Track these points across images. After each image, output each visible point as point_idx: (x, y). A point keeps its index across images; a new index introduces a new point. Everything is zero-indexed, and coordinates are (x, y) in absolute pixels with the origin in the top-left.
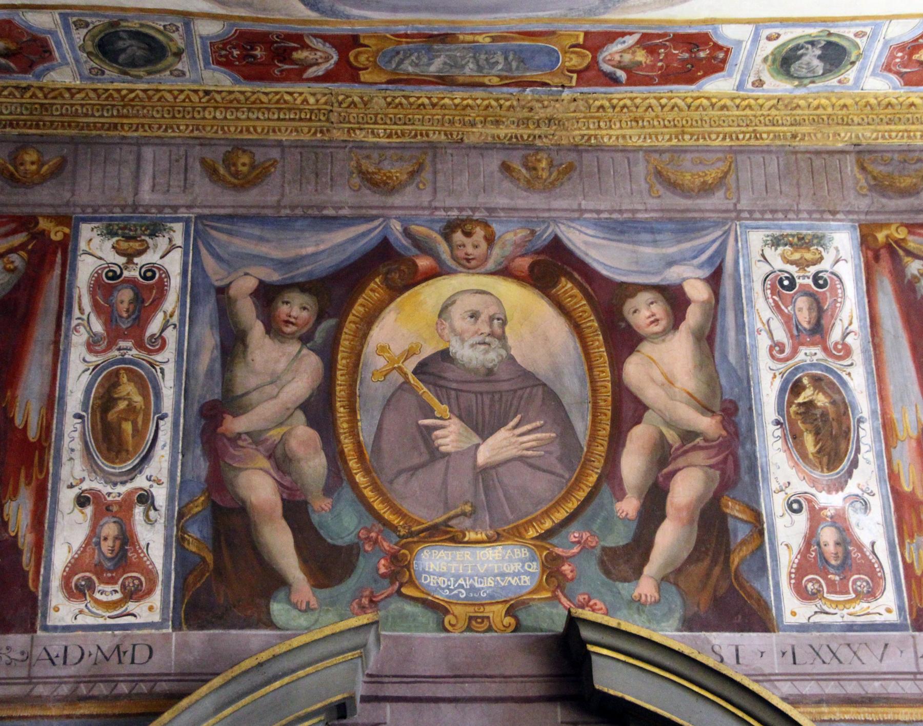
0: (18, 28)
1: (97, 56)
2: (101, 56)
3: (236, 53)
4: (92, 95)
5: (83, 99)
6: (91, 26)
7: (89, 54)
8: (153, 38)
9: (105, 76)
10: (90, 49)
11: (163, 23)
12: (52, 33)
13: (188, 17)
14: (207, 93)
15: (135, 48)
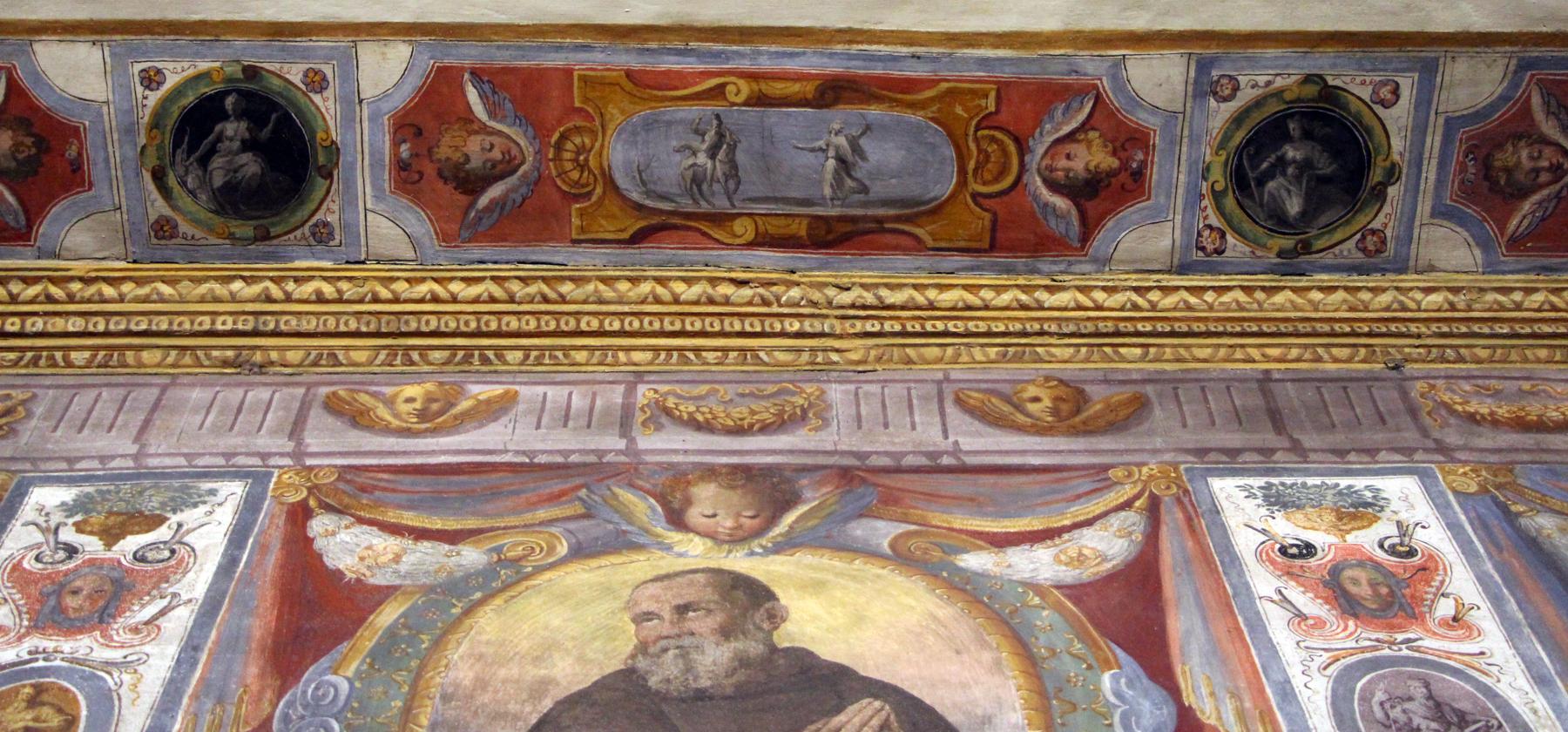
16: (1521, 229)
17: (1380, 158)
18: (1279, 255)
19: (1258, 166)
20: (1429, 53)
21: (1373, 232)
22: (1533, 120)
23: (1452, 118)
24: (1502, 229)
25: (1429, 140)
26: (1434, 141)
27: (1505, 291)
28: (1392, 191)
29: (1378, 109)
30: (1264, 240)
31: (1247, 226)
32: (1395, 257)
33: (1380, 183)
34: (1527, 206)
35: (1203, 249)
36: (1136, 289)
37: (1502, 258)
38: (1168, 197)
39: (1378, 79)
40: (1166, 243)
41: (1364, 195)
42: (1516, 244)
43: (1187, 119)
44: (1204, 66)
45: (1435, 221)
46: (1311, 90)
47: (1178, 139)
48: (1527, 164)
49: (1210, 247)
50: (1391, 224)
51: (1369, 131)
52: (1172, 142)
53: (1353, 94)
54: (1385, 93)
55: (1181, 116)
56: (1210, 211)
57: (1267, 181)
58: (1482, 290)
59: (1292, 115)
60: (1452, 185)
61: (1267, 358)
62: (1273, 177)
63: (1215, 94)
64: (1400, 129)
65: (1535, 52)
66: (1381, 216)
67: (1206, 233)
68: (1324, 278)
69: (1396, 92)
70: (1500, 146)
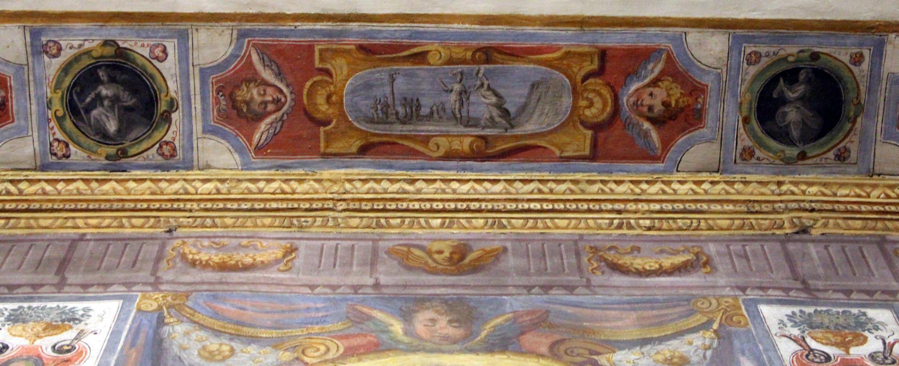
16: (262, 141)
17: (163, 95)
18: (107, 158)
19: (83, 101)
20: (182, 26)
21: (167, 143)
22: (255, 70)
23: (204, 69)
24: (250, 140)
25: (192, 82)
26: (195, 83)
27: (255, 181)
28: (175, 116)
29: (155, 62)
30: (95, 149)
31: (82, 139)
32: (184, 159)
33: (165, 111)
34: (263, 126)
35: (55, 154)
36: (11, 181)
37: (253, 160)
38: (26, 119)
39: (152, 43)
40: (29, 151)
41: (156, 116)
42: (260, 150)
43: (31, 69)
44: (35, 34)
45: (206, 136)
46: (109, 51)
47: (27, 83)
48: (258, 99)
49: (60, 154)
50: (177, 138)
51: (152, 76)
52: (23, 85)
53: (138, 53)
54: (158, 52)
55: (26, 68)
56: (56, 130)
57: (91, 110)
58: (239, 181)
59: (100, 67)
60: (213, 114)
61: (88, 226)
62: (95, 107)
63: (47, 53)
64: (172, 76)
65: (248, 26)
66: (170, 132)
67: (56, 144)
68: (138, 173)
69: (165, 51)
70: (238, 87)
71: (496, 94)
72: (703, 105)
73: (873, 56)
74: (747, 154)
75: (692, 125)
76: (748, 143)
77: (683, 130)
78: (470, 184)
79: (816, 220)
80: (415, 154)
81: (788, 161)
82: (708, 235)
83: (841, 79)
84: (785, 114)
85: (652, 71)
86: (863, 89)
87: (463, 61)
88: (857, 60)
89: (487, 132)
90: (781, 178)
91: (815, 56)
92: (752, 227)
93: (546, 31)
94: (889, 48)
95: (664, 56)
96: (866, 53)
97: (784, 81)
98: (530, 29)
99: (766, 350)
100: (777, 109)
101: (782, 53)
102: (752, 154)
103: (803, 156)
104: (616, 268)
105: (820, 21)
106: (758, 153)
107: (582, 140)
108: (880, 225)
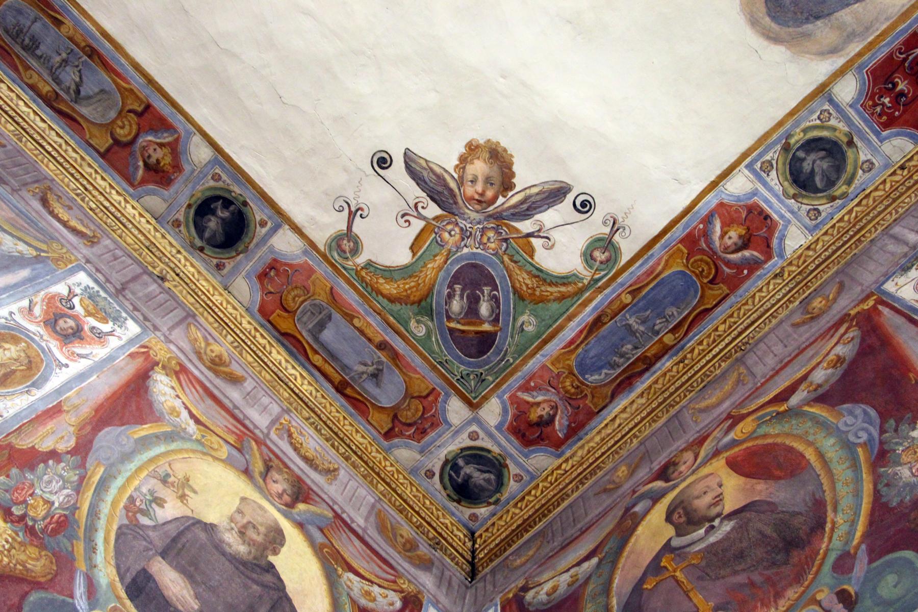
0: (731, 206)
1: (803, 197)
2: (804, 193)
3: (887, 100)
4: (826, 238)
5: (823, 246)
6: (774, 163)
7: (794, 197)
8: (820, 139)
9: (824, 214)
10: (792, 191)
11: (815, 116)
12: (755, 193)
13: (823, 91)
14: (902, 168)
15: (818, 162)
71: (81, 78)
72: (175, 179)
73: (271, 229)
74: (177, 224)
75: (162, 184)
76: (182, 219)
77: (156, 183)
78: (30, 110)
79: (174, 280)
80: (16, 70)
81: (192, 245)
82: (115, 238)
83: (248, 226)
84: (210, 220)
85: (164, 138)
86: (255, 241)
87: (77, 45)
88: (263, 224)
89: (61, 93)
90: (182, 250)
91: (245, 204)
92: (140, 255)
93: (130, 68)
94: (281, 231)
95: (176, 136)
96: (269, 224)
97: (222, 203)
98: (123, 61)
99: (48, 280)
100: (207, 214)
101: (231, 188)
102: (179, 226)
103: (201, 249)
104: (44, 202)
105: (260, 188)
106: (182, 228)
107: (104, 142)
108: (201, 310)
